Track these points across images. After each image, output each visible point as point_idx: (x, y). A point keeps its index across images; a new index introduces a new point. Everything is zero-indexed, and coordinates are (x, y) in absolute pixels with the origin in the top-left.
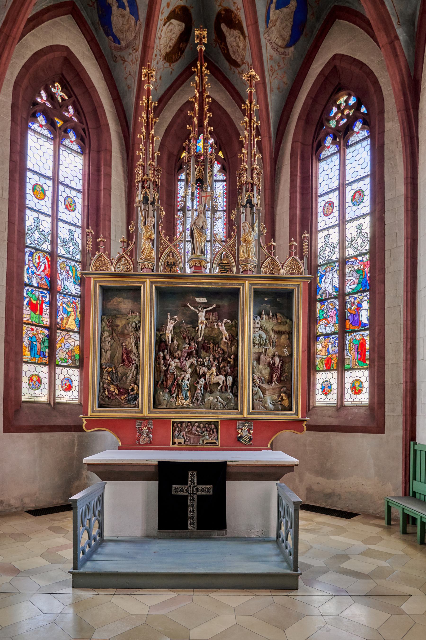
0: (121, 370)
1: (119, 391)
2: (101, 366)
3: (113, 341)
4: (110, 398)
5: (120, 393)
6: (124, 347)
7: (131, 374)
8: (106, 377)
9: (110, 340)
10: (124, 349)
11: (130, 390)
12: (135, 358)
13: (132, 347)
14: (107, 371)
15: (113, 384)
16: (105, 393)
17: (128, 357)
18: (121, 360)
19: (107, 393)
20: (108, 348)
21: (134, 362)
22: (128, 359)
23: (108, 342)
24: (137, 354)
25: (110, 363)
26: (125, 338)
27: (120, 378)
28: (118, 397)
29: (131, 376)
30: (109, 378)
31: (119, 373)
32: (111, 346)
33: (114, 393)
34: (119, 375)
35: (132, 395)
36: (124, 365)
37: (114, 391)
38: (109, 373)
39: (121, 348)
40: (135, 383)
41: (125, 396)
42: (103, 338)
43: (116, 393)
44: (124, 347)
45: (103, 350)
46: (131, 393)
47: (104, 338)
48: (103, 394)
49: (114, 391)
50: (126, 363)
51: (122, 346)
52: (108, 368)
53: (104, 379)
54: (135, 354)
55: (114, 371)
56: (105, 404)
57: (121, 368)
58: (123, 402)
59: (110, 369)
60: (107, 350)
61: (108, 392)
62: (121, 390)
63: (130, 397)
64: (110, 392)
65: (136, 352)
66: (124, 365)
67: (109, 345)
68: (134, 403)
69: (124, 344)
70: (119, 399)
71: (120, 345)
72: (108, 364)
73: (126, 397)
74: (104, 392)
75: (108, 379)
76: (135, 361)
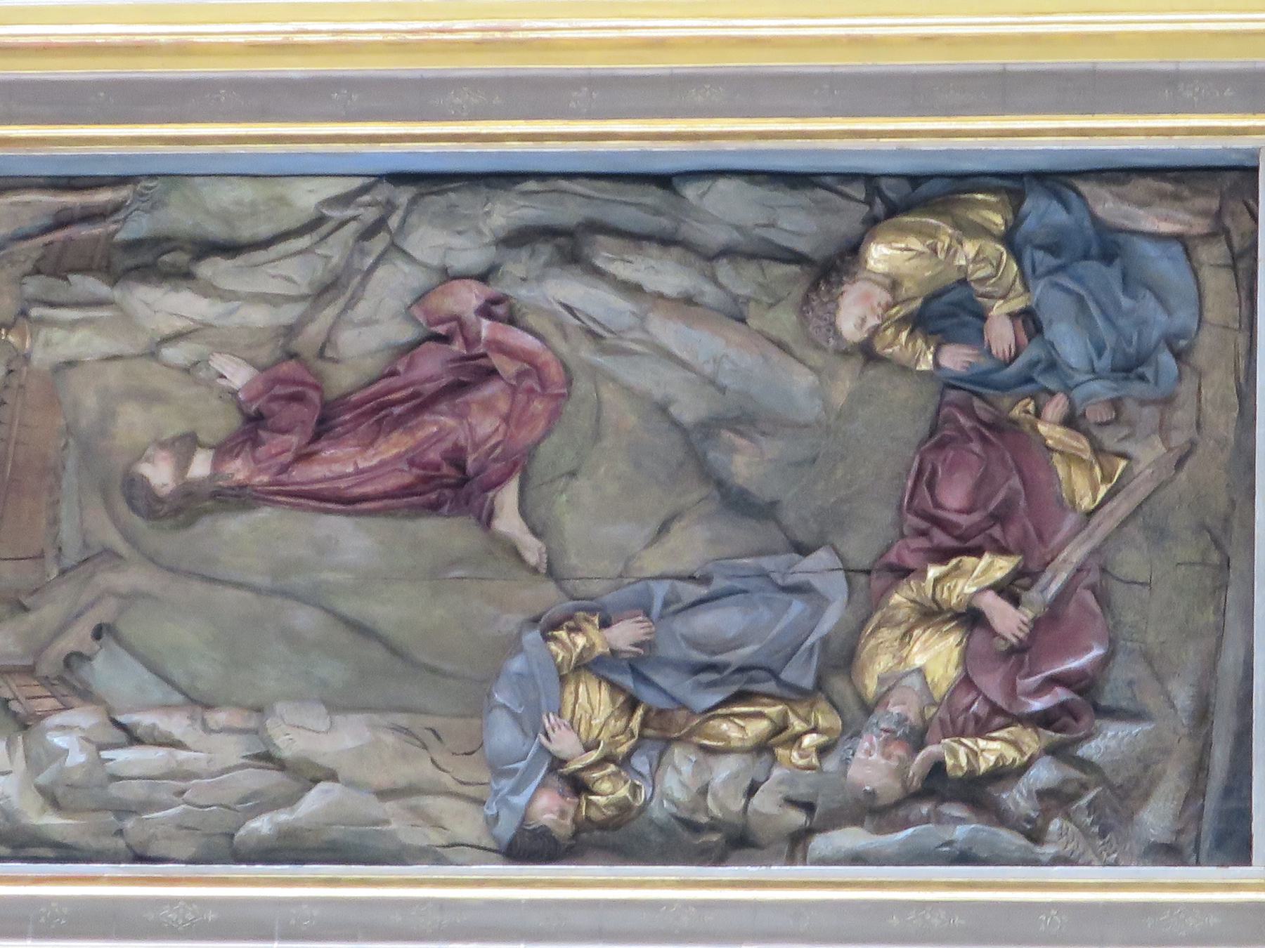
0: (602, 518)
1: (970, 546)
2: (531, 847)
3: (112, 673)
4: (1084, 685)
5: (1012, 521)
6: (201, 466)
7: (668, 331)
8: (724, 769)
9: (84, 718)
10: (238, 470)
11: (956, 358)
12: (392, 285)
13: (216, 328)
14: (624, 762)
15: (843, 657)
16: (1003, 774)
17: (381, 407)
18: (445, 533)
19: (992, 751)
20: (231, 750)
21: (467, 299)
22: (424, 404)
23: (133, 738)
24: (335, 250)
25: (480, 707)
26: (53, 472)
27: (744, 534)
28: (1075, 554)
29: (703, 344)
30: (743, 729)
31: (653, 562)
32: (198, 703)
33: (1009, 621)
34: (690, 546)
35: (1029, 321)
36: (517, 463)
37: (972, 619)
38: (660, 731)
39: (235, 525)
40: (834, 267)
41: (1051, 431)
42: (52, 822)
43: (1009, 590)
44: (201, 466)
45: (262, 825)
46: (1001, 333)
47: (53, 800)
48: (1017, 798)
49: (972, 619)
50: (486, 425)
51: (189, 505)
52: (564, 743)
53: (764, 802)
54: (326, 290)
55: (625, 634)
56: (1200, 769)
57: (571, 524)
58: (1148, 454)
59: (594, 703)
60: (267, 759)
61: (982, 728)
62: (953, 496)
63: (1069, 343)
64: (991, 684)
65: (289, 272)
66: (517, 463)
67: (176, 725)
68: (1164, 266)
69: (160, 474)
70: (1104, 525)
71: (169, 542)
72: (503, 734)
73: (1071, 421)
74: (978, 791)
75: (763, 748)
76: (448, 276)
